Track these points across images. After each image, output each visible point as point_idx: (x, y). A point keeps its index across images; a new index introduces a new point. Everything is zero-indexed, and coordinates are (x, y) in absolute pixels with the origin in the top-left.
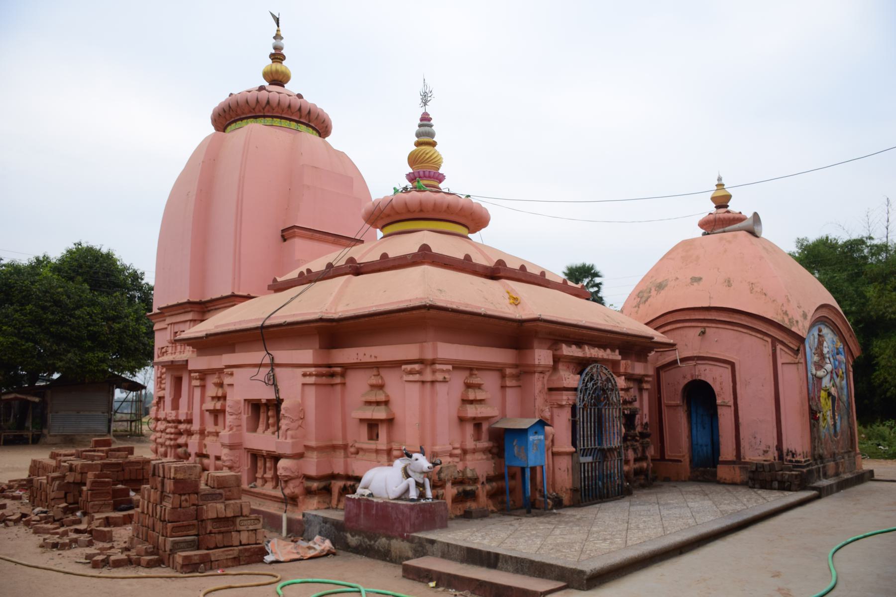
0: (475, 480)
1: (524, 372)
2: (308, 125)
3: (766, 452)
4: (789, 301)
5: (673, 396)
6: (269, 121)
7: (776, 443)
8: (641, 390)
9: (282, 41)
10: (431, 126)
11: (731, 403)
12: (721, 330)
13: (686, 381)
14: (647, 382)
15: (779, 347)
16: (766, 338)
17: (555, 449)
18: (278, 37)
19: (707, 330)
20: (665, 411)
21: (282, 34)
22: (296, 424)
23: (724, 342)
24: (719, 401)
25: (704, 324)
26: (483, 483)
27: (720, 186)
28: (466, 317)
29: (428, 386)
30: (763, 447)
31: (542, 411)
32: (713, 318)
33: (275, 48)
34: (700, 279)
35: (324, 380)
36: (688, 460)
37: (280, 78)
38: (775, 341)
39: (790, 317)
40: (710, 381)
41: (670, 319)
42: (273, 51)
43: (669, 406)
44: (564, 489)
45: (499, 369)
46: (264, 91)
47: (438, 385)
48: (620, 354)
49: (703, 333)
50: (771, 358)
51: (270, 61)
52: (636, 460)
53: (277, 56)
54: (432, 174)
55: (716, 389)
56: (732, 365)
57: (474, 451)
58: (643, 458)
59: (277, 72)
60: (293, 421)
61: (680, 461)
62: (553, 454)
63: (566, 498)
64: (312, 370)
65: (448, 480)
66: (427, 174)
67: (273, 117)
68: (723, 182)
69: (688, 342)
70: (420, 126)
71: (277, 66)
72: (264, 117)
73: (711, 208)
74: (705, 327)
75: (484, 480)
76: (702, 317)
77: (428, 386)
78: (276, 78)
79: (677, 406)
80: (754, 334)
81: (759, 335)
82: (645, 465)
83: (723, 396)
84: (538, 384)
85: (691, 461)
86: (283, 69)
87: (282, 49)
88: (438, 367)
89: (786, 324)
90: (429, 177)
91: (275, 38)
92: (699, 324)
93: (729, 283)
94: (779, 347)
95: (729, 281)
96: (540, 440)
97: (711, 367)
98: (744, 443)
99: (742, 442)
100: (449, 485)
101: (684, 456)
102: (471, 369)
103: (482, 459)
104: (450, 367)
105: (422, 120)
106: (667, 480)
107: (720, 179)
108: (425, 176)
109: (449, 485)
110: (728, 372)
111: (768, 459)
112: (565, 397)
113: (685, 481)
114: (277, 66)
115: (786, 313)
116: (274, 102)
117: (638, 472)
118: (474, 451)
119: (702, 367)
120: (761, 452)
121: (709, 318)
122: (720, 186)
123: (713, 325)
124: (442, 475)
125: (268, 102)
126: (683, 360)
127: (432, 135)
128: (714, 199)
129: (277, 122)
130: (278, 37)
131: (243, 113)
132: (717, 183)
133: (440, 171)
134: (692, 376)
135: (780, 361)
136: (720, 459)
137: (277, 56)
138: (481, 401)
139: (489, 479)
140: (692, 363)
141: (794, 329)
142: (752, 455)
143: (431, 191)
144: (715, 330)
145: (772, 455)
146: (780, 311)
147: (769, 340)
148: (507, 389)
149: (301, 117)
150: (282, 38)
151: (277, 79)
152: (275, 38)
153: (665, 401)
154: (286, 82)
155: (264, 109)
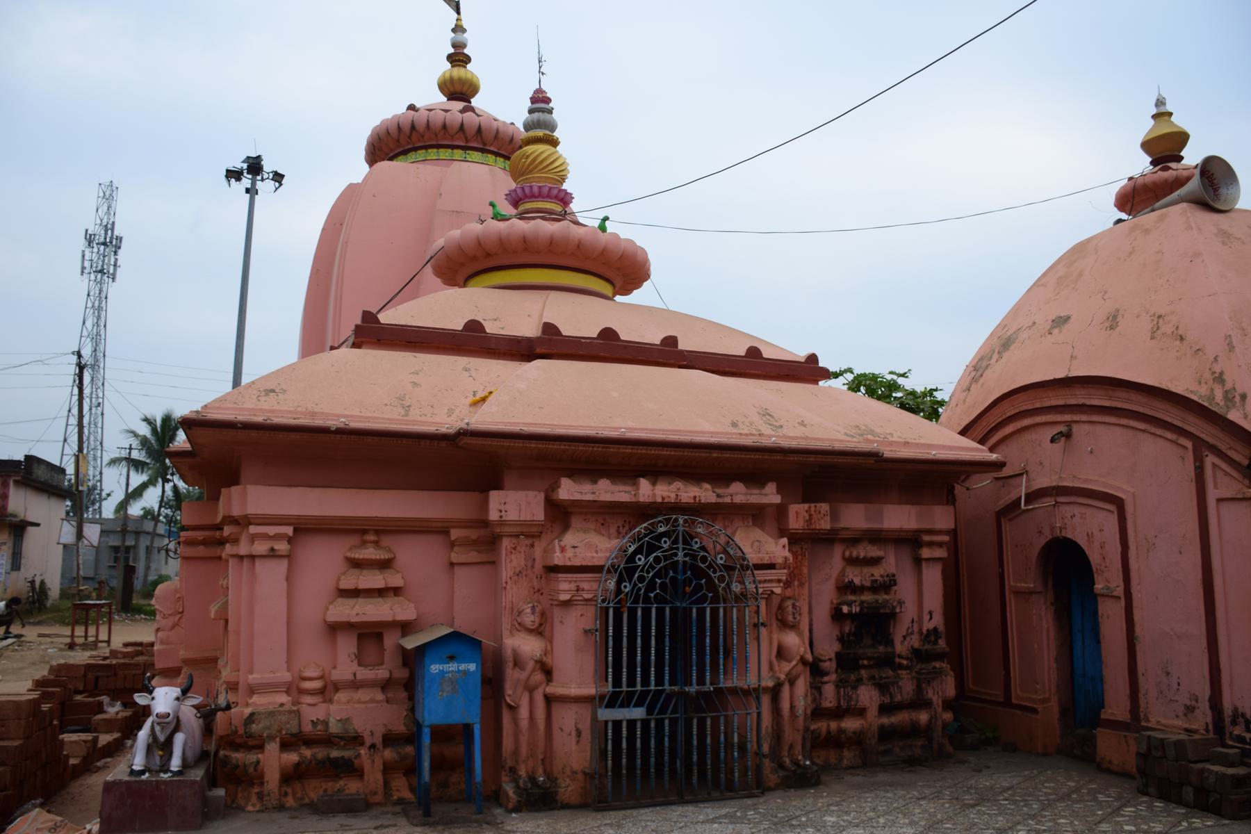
0: (357, 740)
1: (488, 539)
2: (483, 151)
3: (1190, 709)
4: (1231, 347)
5: (1022, 573)
6: (421, 154)
7: (1207, 693)
8: (918, 561)
9: (465, 35)
10: (550, 111)
11: (1120, 591)
12: (1099, 428)
13: (1043, 541)
14: (931, 544)
15: (1210, 459)
16: (1183, 441)
17: (549, 690)
18: (458, 29)
19: (1075, 428)
20: (1011, 600)
21: (465, 24)
22: (171, 621)
23: (1110, 457)
24: (1098, 587)
25: (1067, 417)
26: (373, 746)
27: (1162, 115)
28: (293, 436)
29: (246, 562)
30: (1184, 699)
31: (520, 613)
32: (1081, 401)
33: (454, 46)
34: (1069, 318)
35: (201, 551)
36: (1056, 709)
37: (465, 88)
38: (1200, 448)
39: (1229, 385)
40: (1082, 542)
41: (1009, 409)
42: (452, 51)
43: (1017, 593)
44: (568, 772)
45: (438, 529)
46: (470, 114)
47: (259, 564)
48: (778, 492)
49: (1068, 435)
50: (1193, 486)
51: (448, 65)
52: (884, 709)
53: (458, 58)
54: (545, 191)
55: (1094, 557)
56: (1118, 503)
57: (356, 685)
58: (919, 703)
59: (460, 80)
60: (164, 617)
61: (1034, 711)
62: (549, 700)
63: (568, 789)
64: (199, 535)
65: (272, 738)
66: (536, 190)
67: (426, 147)
68: (1169, 107)
69: (1040, 459)
70: (531, 111)
71: (458, 72)
72: (415, 149)
73: (1140, 164)
74: (1069, 424)
75: (378, 740)
76: (1061, 402)
77: (246, 562)
78: (458, 88)
79: (1031, 593)
80: (1159, 432)
81: (1169, 435)
82: (923, 717)
83: (1107, 579)
84: (511, 559)
85: (1064, 712)
86: (469, 76)
87: (464, 46)
88: (253, 529)
89: (1217, 403)
90: (549, 196)
91: (454, 30)
92: (1059, 418)
93: (1113, 321)
94: (1210, 459)
95: (1115, 317)
96: (466, 673)
97: (1083, 510)
98: (1147, 685)
99: (1141, 680)
100: (272, 748)
101: (1043, 701)
102: (377, 532)
103: (373, 701)
104: (289, 530)
105: (534, 100)
106: (1012, 748)
107: (1160, 102)
108: (526, 196)
109: (272, 748)
110: (1112, 521)
111: (1194, 727)
112: (564, 586)
113: (1044, 755)
114: (458, 72)
115: (1220, 379)
116: (421, 127)
117: (886, 734)
118: (356, 685)
119: (1067, 511)
120: (1181, 710)
121: (1073, 402)
122: (1162, 115)
123: (1084, 418)
124: (254, 728)
125: (413, 127)
126: (1032, 497)
127: (552, 127)
128: (1147, 146)
129: (432, 153)
130: (458, 29)
131: (391, 150)
132: (1154, 111)
133: (565, 186)
134: (1052, 529)
135: (1212, 494)
136: (1103, 716)
137: (458, 58)
138: (397, 591)
139: (390, 739)
140: (1049, 501)
141: (1234, 416)
142: (1168, 718)
143: (543, 218)
144: (1087, 427)
145: (1203, 717)
146: (1208, 375)
147: (1189, 444)
148: (456, 568)
149: (467, 141)
150: (464, 31)
151: (459, 91)
152: (454, 30)
153: (1011, 582)
154: (473, 96)
155: (410, 137)
